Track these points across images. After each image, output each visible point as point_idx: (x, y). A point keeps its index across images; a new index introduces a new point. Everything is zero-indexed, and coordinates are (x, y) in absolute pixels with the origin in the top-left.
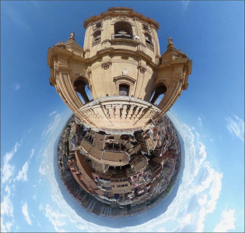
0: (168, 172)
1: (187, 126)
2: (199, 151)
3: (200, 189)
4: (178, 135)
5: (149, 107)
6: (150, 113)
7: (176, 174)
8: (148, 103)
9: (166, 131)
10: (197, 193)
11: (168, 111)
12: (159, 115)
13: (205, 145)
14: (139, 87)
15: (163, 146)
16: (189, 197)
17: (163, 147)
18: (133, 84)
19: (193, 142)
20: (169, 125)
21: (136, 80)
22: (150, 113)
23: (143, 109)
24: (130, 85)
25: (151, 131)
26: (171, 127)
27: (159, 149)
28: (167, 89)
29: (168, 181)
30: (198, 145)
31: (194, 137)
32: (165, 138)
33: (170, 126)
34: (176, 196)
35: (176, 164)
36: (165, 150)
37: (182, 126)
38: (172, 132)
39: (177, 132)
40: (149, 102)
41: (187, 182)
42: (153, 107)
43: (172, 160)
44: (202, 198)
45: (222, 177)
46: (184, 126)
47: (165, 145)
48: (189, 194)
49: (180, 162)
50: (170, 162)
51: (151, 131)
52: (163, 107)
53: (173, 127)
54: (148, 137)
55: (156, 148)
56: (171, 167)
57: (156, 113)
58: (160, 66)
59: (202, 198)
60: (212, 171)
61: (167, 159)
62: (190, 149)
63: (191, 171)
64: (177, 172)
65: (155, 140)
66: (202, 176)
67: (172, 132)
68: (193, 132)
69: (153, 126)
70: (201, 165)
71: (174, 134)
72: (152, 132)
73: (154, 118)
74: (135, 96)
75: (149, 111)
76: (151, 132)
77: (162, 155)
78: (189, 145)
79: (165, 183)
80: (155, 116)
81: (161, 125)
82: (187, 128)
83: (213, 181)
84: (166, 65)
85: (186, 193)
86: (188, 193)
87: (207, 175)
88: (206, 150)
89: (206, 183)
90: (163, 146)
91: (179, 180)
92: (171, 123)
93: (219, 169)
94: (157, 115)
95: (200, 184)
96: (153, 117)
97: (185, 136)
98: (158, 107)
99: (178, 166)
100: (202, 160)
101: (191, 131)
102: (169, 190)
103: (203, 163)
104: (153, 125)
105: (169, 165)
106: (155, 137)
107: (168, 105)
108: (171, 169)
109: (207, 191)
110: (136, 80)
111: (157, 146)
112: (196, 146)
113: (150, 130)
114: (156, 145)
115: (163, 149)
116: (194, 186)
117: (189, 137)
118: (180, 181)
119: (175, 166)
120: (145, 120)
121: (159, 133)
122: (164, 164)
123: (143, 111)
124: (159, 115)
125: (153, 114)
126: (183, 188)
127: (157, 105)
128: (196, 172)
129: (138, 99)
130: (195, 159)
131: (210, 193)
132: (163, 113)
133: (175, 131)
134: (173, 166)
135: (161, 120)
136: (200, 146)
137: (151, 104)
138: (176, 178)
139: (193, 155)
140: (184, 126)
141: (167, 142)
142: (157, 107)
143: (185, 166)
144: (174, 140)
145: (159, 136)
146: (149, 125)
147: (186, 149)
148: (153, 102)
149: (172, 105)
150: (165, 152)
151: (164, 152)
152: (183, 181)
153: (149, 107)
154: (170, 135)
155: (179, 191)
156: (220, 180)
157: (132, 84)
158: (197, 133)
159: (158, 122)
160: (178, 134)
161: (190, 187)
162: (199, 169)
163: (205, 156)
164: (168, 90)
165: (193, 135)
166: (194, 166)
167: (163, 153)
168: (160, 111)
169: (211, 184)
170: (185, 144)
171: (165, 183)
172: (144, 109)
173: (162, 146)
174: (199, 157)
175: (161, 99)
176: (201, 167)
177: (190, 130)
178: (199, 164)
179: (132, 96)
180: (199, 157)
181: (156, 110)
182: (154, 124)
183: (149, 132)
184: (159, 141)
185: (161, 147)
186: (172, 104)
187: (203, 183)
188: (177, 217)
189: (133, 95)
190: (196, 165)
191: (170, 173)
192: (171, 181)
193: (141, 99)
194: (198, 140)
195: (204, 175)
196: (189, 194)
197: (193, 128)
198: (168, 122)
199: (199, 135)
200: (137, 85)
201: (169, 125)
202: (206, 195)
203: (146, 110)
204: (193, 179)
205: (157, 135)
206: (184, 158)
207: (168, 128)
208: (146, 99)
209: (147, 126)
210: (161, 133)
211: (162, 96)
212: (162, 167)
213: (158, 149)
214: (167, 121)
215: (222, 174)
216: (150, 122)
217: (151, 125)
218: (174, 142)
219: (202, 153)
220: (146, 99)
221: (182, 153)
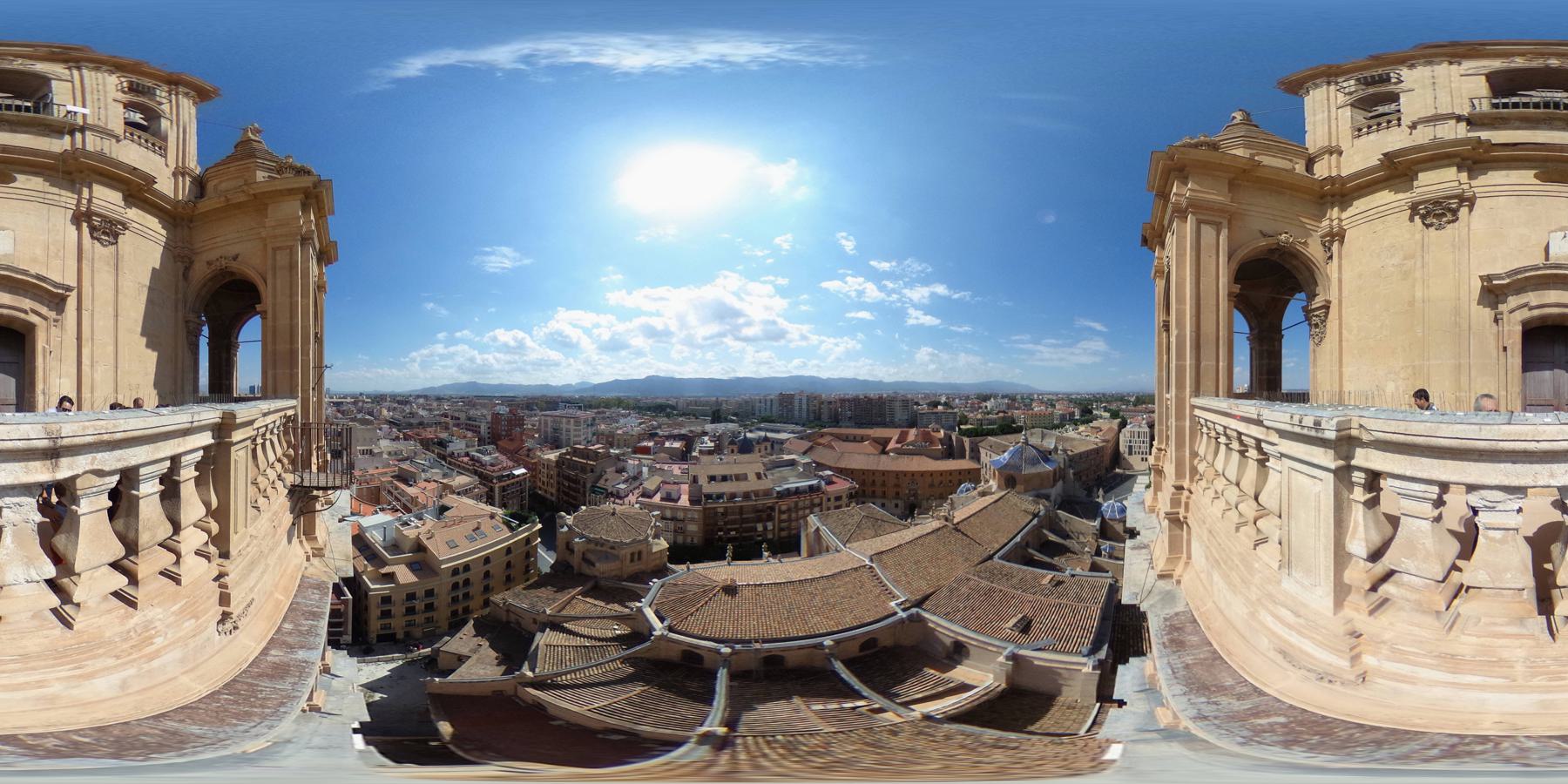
0: (572, 427)
1: (425, 352)
2: (506, 345)
3: (586, 343)
4: (442, 394)
5: (222, 429)
6: (255, 456)
7: (569, 402)
8: (196, 408)
9: (405, 439)
10: (595, 346)
11: (327, 374)
12: (306, 428)
13: (496, 329)
14: (99, 322)
15: (476, 468)
16: (606, 358)
17: (483, 465)
18: (52, 315)
19: (479, 354)
20: (385, 412)
21: (73, 283)
22: (255, 456)
23: (188, 473)
24: (31, 327)
25: (375, 527)
27: (490, 488)
28: (261, 288)
29: (596, 413)
30: (491, 343)
31: (466, 347)
32: (439, 455)
33: (389, 411)
34: (616, 380)
35: (541, 410)
36: (497, 458)
37: (416, 365)
38: (421, 412)
39: (428, 394)
40: (203, 400)
41: (579, 370)
42: (243, 412)
43: (530, 426)
44: (599, 336)
45: (564, 309)
46: (418, 359)
47: (472, 459)
48: (600, 359)
49: (534, 398)
50: (538, 431)
51: (376, 522)
52: (293, 376)
53: (402, 400)
54: (419, 547)
55: (490, 500)
56: (554, 421)
57: (286, 433)
58: (199, 206)
59: (599, 336)
60: (553, 325)
61: (529, 444)
62: (496, 366)
63: (552, 368)
64: (562, 402)
65: (443, 509)
66: (562, 343)
67: (421, 412)
68: (451, 341)
69: (343, 499)
70: (540, 345)
71: (430, 410)
72: (383, 518)
73: (299, 463)
74: (86, 394)
75: (239, 456)
76: (384, 527)
77: (519, 466)
78: (485, 369)
79: (603, 418)
80: (295, 448)
81: (363, 452)
82: (432, 355)
83: (570, 324)
84: (228, 200)
85: (601, 365)
86: (601, 362)
87: (560, 334)
88: (509, 329)
89: (574, 334)
90: (476, 468)
91: (585, 390)
92: (379, 399)
93: (550, 313)
94: (298, 433)
95: (578, 343)
96: (293, 462)
97: (451, 371)
98: (269, 390)
99: (547, 402)
100: (529, 342)
101: (446, 347)
102: (613, 399)
103: (534, 341)
104: (333, 495)
105: (549, 430)
106: (425, 507)
107: (306, 353)
108: (561, 422)
109: (587, 332)
110: (69, 289)
111: (478, 498)
112: (493, 349)
113: (360, 526)
114: (471, 502)
115: (492, 465)
116: (585, 355)
117: (460, 360)
118: (583, 387)
119: (548, 413)
120: (263, 523)
121: (405, 478)
122: (552, 449)
123: (199, 482)
124: (306, 428)
125: (276, 450)
126: (594, 374)
127: (252, 389)
128: (554, 355)
129: (117, 413)
130: (525, 358)
131: (590, 326)
132: (313, 399)
133: (421, 401)
134: (549, 418)
135: (340, 434)
136: (495, 339)
137: (221, 401)
138: (579, 399)
139: (515, 362)
140: (418, 359)
141: (457, 446)
142: (264, 397)
143: (544, 383)
145: (422, 484)
146: (325, 522)
147: (493, 379)
148: (221, 387)
149: (319, 340)
150: (502, 458)
151: (505, 461)
152: (579, 381)
153: (222, 429)
155: (604, 380)
156: (569, 312)
157: (45, 318)
158: (458, 334)
159: (337, 455)
160: (436, 393)
161: (588, 362)
162: (548, 350)
163: (521, 335)
164: (266, 292)
165: (460, 348)
166: (542, 360)
167: (510, 464)
168: (290, 405)
169: (575, 326)
171: (603, 418)
172: (199, 466)
173: (476, 473)
174: (520, 347)
175: (258, 347)
176: (544, 346)
177: (440, 349)
178: (536, 349)
179: (64, 399)
180: (520, 347)
181: (269, 419)
182: (335, 488)
183: (376, 538)
184: (447, 488)
185: (481, 475)
186: (316, 334)
187: (575, 340)
188: (645, 356)
189: (73, 396)
190: (540, 357)
191: (572, 420)
192: (589, 407)
193: (137, 404)
194: (477, 339)
195: (560, 339)
196: (600, 359)
197: (441, 336)
198: (366, 407)
199: (466, 332)
200: (85, 315)
201: (385, 412)
202: (595, 331)
203: (214, 465)
204: (571, 360)
205: (411, 491)
206: (521, 386)
207: (392, 423)
208: (174, 390)
209: (320, 532)
210: (406, 466)
211: (251, 333)
212: (564, 451)
213: (492, 489)
214: (360, 411)
215: (560, 308)
216: (303, 502)
217: (330, 503)
219: (513, 339)
220: (174, 390)
221: (507, 395)
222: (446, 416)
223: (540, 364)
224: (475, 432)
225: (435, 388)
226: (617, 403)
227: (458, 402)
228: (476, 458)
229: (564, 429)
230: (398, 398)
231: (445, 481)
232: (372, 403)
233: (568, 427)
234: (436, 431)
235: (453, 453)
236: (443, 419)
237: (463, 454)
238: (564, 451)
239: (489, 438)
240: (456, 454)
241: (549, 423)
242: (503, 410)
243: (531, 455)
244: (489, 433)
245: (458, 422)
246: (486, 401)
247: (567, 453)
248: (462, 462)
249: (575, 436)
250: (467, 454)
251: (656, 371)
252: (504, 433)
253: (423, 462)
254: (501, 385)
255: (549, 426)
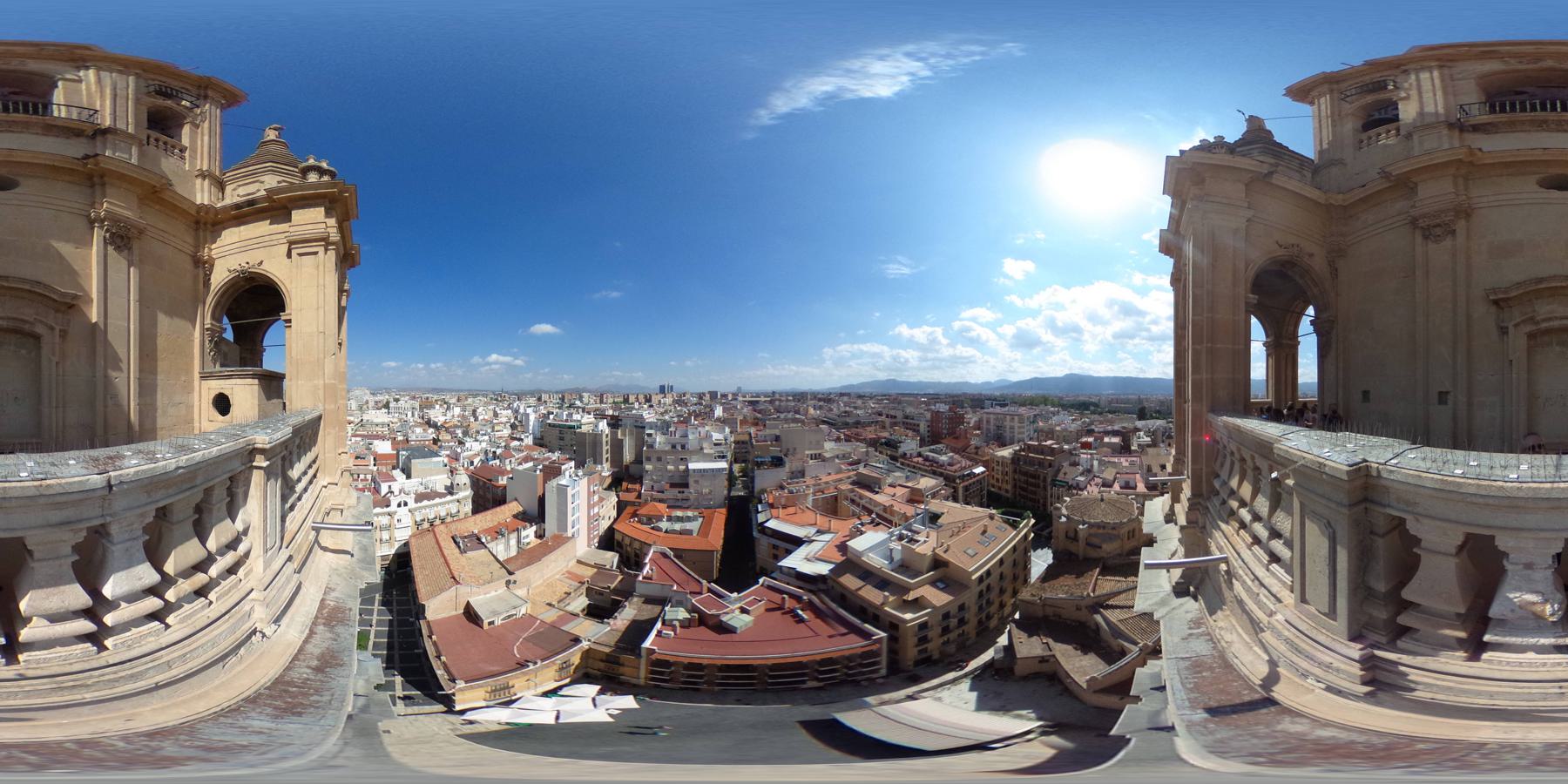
0: (1016, 424)
105: (992, 427)
144: (892, 413)
154: (869, 424)
170: (899, 379)
191: (1016, 418)
206: (940, 384)
218: (899, 414)
223: (956, 361)
224: (914, 430)
226: (1043, 400)
227: (883, 400)
228: (931, 458)
229: (1008, 427)
230: (820, 396)
232: (794, 400)
233: (1012, 424)
234: (875, 431)
235: (905, 454)
236: (880, 419)
237: (915, 454)
238: (1018, 448)
239: (928, 437)
240: (908, 455)
241: (992, 421)
242: (943, 408)
243: (980, 453)
244: (929, 431)
245: (894, 420)
246: (911, 399)
247: (1020, 450)
248: (918, 463)
250: (919, 455)
251: (1070, 369)
252: (945, 431)
253: (880, 466)
254: (921, 383)
255: (992, 424)
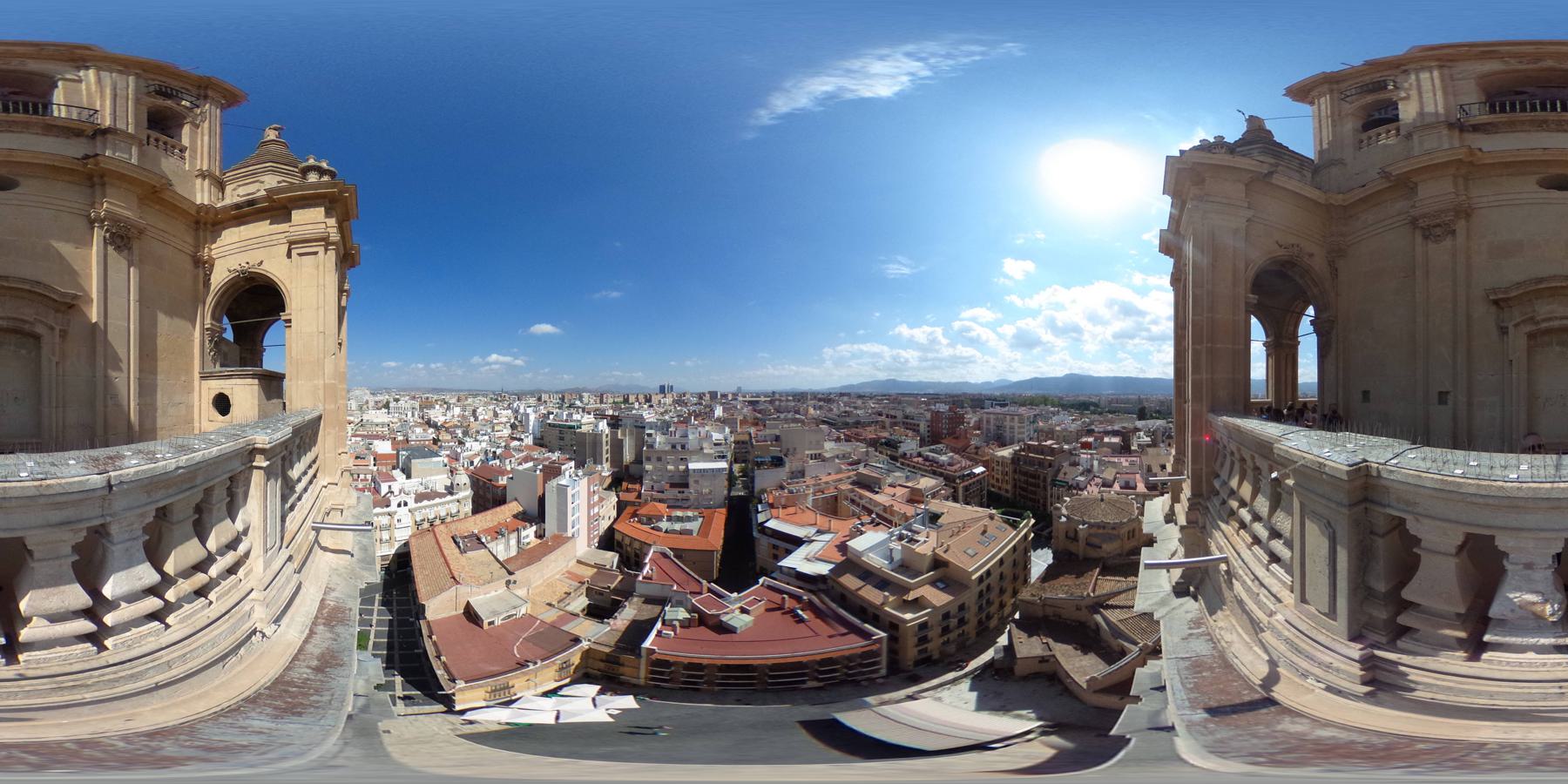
0: (1016, 424)
9: (846, 441)
20: (811, 411)
26: (820, 408)
33: (815, 409)
34: (1036, 378)
77: (977, 463)
92: (801, 397)
173: (934, 473)
201: (811, 411)
222: (880, 415)
225: (853, 385)
228: (931, 458)
231: (909, 484)
240: (908, 455)
248: (918, 463)
249: (1019, 433)
